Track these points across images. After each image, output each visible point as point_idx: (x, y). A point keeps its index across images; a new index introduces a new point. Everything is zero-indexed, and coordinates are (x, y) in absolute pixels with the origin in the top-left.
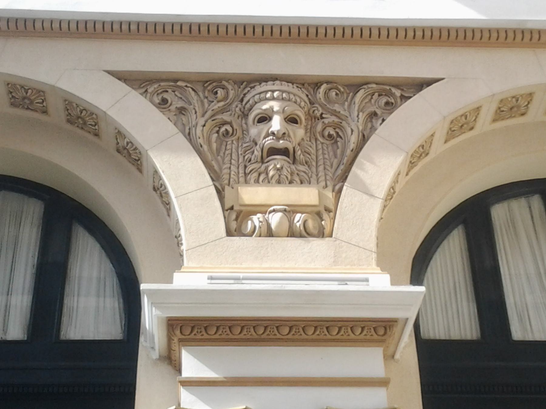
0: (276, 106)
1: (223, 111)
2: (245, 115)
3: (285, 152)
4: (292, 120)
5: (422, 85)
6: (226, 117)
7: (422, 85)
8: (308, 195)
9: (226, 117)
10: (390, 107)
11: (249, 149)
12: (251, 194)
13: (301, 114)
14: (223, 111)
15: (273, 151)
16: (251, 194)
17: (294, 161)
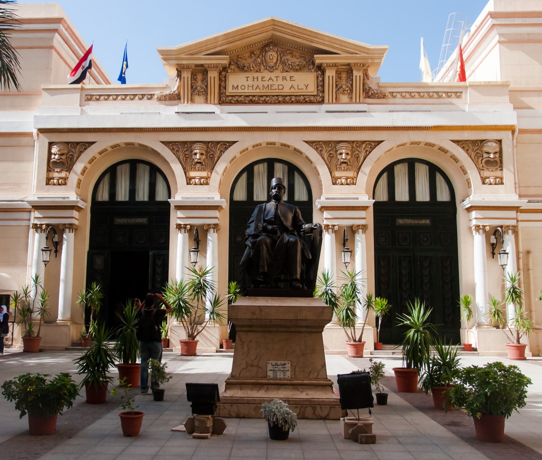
0: (198, 151)
1: (186, 151)
2: (192, 151)
3: (200, 163)
4: (202, 154)
5: (234, 142)
6: (187, 153)
7: (234, 142)
8: (204, 174)
9: (187, 153)
10: (226, 149)
11: (192, 161)
12: (192, 174)
13: (204, 152)
14: (186, 151)
15: (197, 163)
16: (192, 174)
17: (202, 165)
